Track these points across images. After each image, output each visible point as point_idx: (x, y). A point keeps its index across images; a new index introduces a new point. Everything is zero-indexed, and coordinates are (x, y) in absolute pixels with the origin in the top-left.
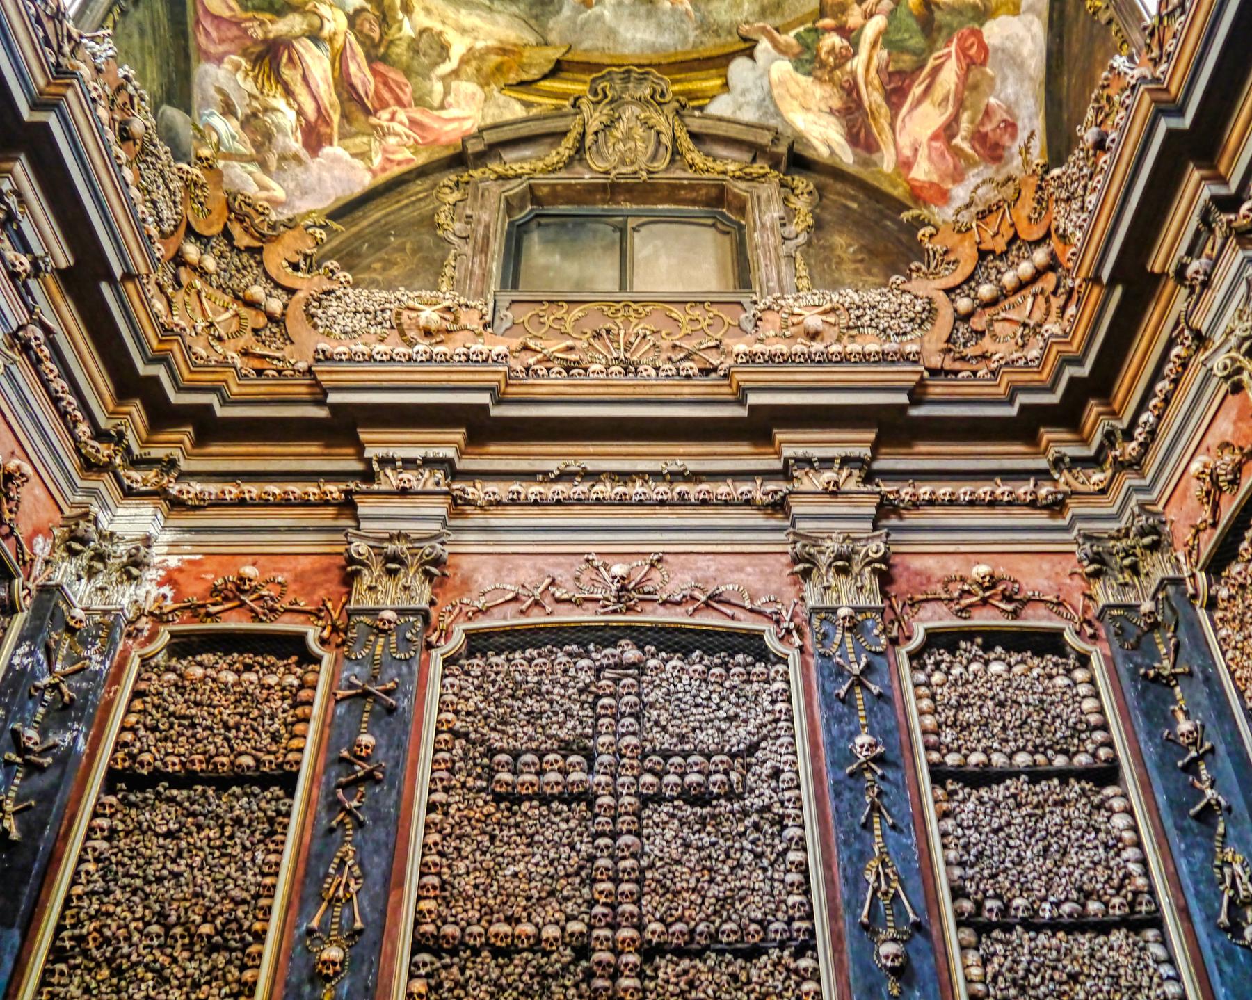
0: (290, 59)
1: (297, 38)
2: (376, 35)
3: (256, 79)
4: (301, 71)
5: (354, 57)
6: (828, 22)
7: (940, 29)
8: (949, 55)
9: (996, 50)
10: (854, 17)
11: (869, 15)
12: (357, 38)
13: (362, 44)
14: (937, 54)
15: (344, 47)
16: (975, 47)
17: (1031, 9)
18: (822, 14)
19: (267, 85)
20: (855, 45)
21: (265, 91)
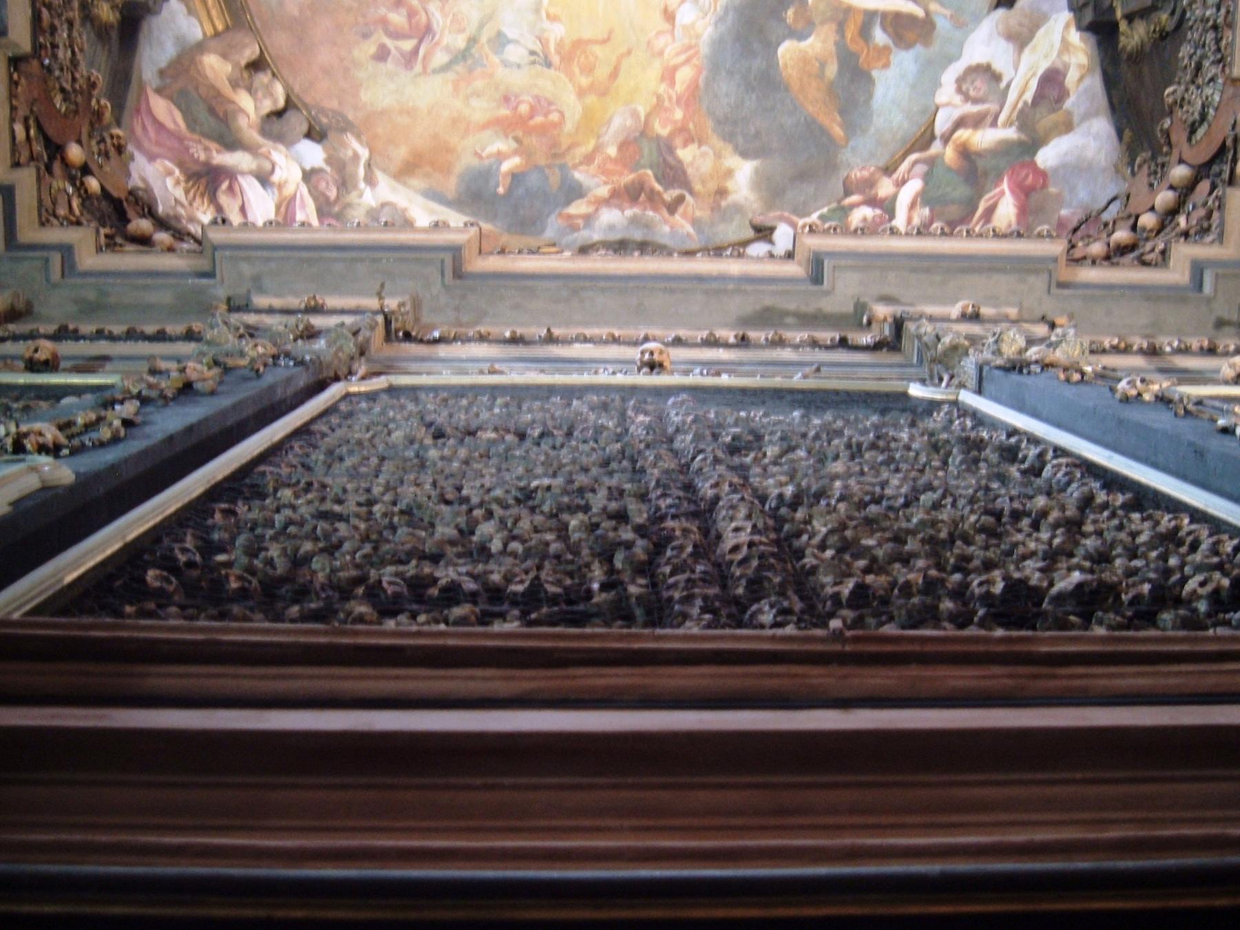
0: (231, 189)
1: (243, 173)
2: (332, 193)
3: (187, 192)
4: (240, 202)
5: (303, 206)
6: (855, 198)
7: (986, 174)
8: (1002, 193)
9: (1055, 170)
10: (885, 188)
11: (903, 182)
12: (310, 191)
13: (315, 199)
14: (987, 197)
15: (294, 198)
16: (1031, 177)
17: (1087, 116)
18: (847, 193)
19: (198, 200)
20: (891, 214)
21: (195, 205)
